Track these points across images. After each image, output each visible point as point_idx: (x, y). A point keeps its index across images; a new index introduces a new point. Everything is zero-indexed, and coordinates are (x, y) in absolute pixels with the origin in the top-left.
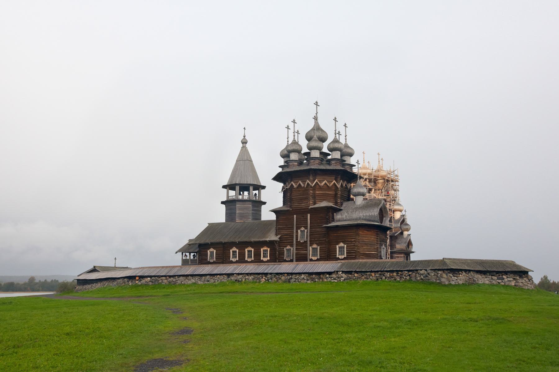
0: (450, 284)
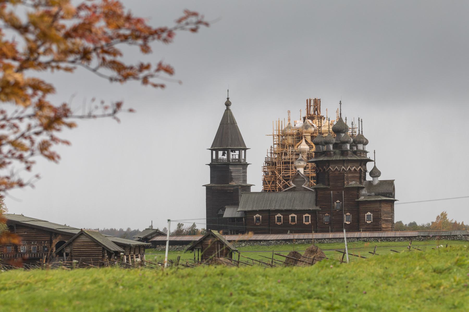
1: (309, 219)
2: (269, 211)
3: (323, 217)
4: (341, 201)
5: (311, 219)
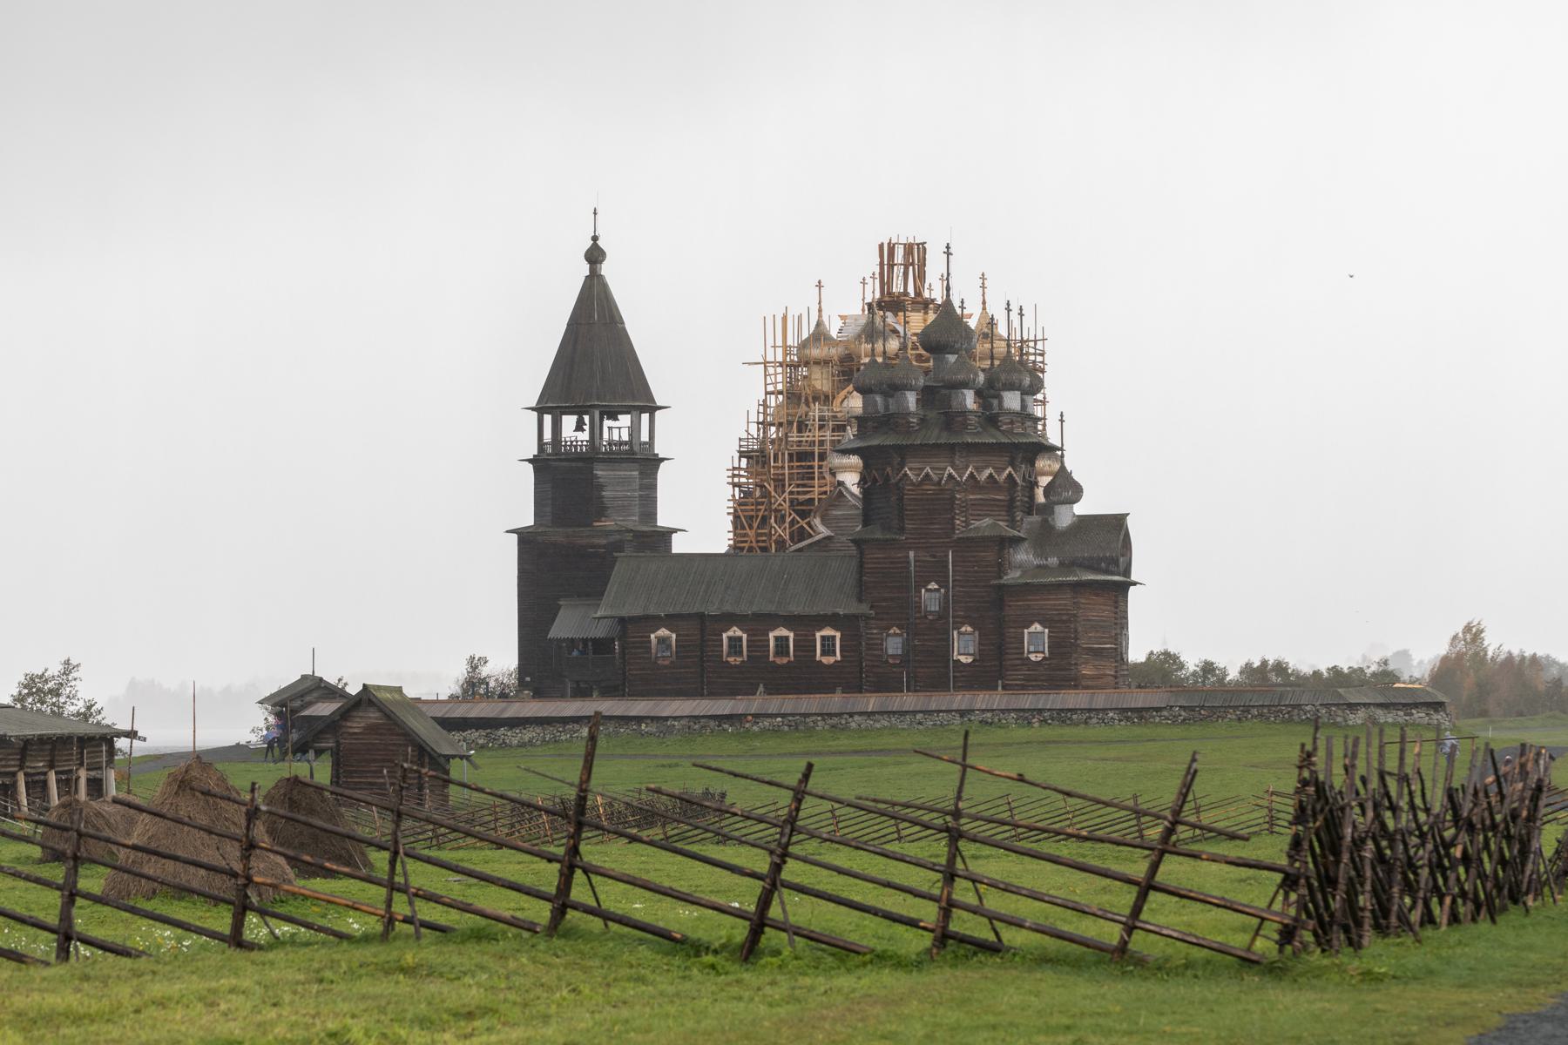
0: (1348, 726)
1: (834, 645)
2: (701, 617)
3: (882, 640)
4: (941, 587)
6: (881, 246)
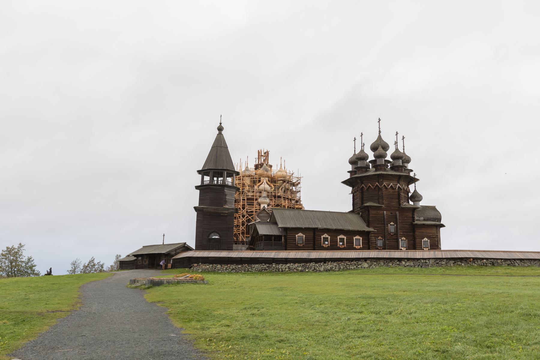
2: (315, 230)
4: (395, 224)
5: (362, 242)
6: (259, 151)
